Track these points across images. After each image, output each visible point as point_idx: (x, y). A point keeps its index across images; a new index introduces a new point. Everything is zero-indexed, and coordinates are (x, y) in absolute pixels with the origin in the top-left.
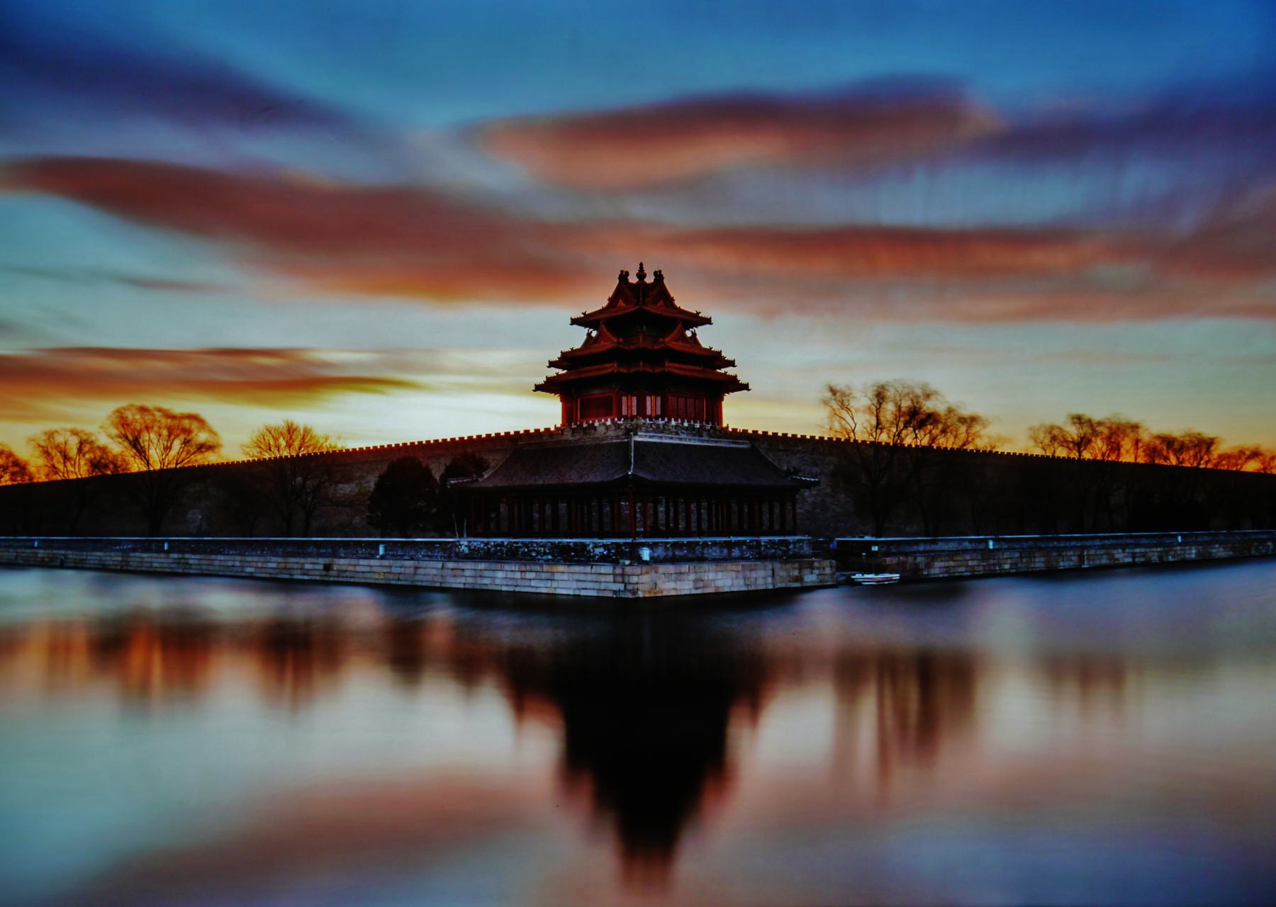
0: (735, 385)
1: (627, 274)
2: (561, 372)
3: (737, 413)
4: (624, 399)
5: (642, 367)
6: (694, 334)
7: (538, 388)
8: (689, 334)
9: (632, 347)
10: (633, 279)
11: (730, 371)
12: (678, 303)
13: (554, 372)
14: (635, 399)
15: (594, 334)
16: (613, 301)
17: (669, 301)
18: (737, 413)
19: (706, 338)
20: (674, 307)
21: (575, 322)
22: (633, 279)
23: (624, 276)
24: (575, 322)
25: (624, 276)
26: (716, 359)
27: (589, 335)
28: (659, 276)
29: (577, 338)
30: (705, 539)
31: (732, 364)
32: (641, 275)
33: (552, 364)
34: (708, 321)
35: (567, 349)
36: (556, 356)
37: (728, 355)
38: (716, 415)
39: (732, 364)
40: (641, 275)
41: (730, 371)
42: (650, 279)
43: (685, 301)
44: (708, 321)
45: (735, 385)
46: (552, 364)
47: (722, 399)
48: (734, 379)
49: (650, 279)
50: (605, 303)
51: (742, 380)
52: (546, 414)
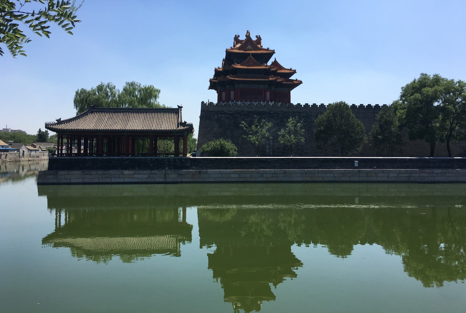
1: (239, 36)
3: (297, 97)
6: (275, 59)
31: (295, 72)
39: (295, 72)
44: (273, 52)
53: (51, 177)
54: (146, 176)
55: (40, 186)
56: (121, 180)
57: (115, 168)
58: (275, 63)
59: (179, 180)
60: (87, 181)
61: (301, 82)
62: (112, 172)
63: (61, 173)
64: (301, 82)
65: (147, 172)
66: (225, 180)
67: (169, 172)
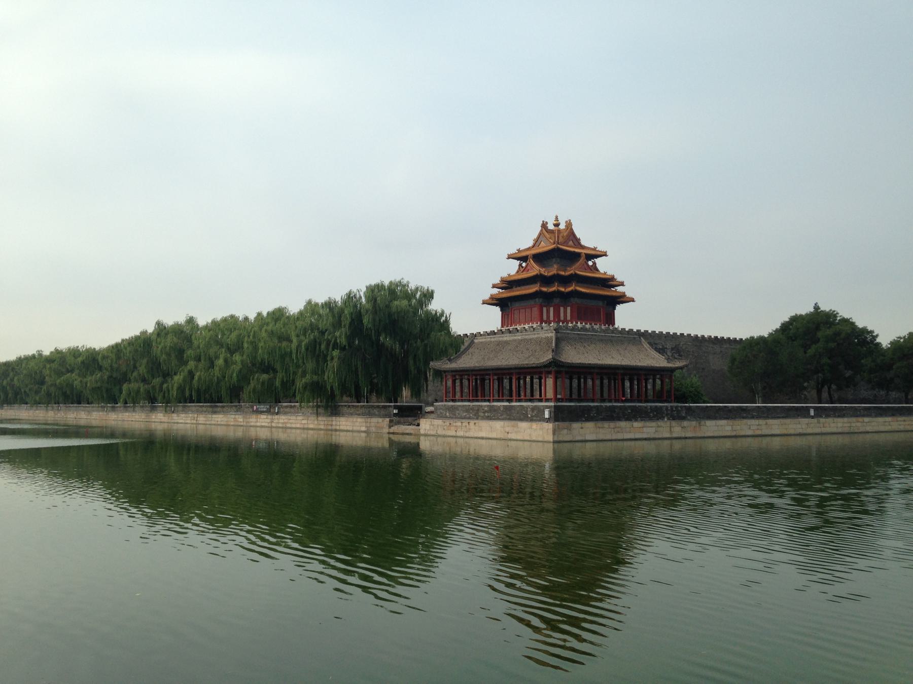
0: (622, 299)
4: (545, 309)
6: (594, 263)
7: (484, 303)
8: (590, 263)
9: (551, 274)
11: (620, 289)
12: (583, 243)
13: (496, 291)
14: (552, 309)
15: (524, 264)
16: (537, 241)
17: (577, 242)
18: (625, 318)
19: (603, 266)
20: (579, 243)
21: (510, 257)
22: (551, 227)
23: (544, 225)
24: (510, 257)
25: (544, 225)
26: (608, 282)
27: (520, 265)
28: (569, 224)
29: (512, 268)
30: (610, 404)
31: (622, 284)
32: (557, 225)
33: (494, 286)
34: (605, 254)
35: (505, 275)
36: (497, 281)
37: (619, 278)
38: (610, 319)
39: (622, 284)
40: (557, 225)
41: (620, 289)
42: (562, 226)
44: (605, 254)
45: (622, 299)
46: (494, 286)
47: (615, 309)
48: (623, 295)
49: (562, 226)
50: (531, 244)
51: (628, 294)
52: (492, 319)
53: (565, 431)
54: (653, 430)
55: (556, 445)
56: (631, 436)
57: (619, 419)
58: (595, 268)
59: (683, 435)
60: (601, 437)
61: (633, 300)
62: (623, 424)
63: (576, 425)
64: (633, 300)
65: (654, 424)
66: (721, 434)
67: (674, 423)
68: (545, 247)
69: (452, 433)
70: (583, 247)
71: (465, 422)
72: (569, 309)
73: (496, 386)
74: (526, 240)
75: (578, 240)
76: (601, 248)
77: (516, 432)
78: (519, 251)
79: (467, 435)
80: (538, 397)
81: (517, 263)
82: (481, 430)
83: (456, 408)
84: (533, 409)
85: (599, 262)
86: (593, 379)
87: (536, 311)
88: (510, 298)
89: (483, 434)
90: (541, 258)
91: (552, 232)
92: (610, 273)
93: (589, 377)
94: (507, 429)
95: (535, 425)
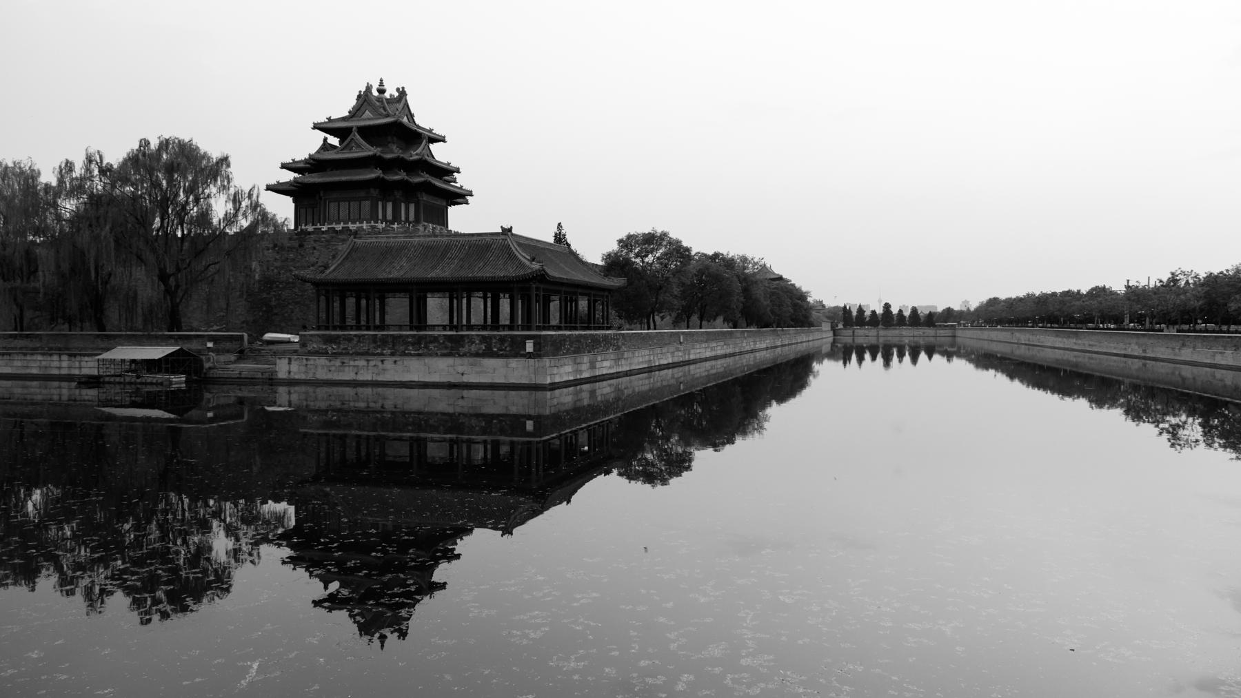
2: (296, 175)
5: (400, 176)
10: (375, 93)
15: (334, 141)
16: (355, 113)
19: (440, 153)
21: (317, 127)
23: (369, 88)
24: (317, 127)
25: (369, 88)
27: (325, 139)
28: (402, 93)
32: (381, 91)
33: (284, 166)
43: (423, 119)
44: (444, 141)
46: (284, 166)
68: (369, 119)
69: (348, 375)
70: (418, 126)
71: (375, 361)
72: (412, 207)
73: (377, 306)
74: (341, 107)
75: (412, 116)
76: (438, 131)
77: (477, 373)
78: (329, 119)
79: (380, 378)
80: (353, 323)
81: (323, 135)
82: (408, 371)
83: (349, 339)
84: (502, 339)
85: (435, 148)
86: (368, 299)
87: (367, 205)
88: (312, 184)
89: (414, 377)
90: (369, 133)
91: (379, 100)
92: (454, 164)
93: (363, 294)
94: (460, 369)
95: (514, 363)
